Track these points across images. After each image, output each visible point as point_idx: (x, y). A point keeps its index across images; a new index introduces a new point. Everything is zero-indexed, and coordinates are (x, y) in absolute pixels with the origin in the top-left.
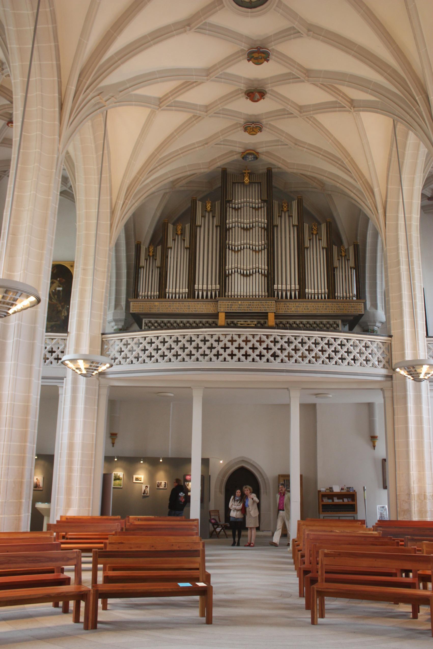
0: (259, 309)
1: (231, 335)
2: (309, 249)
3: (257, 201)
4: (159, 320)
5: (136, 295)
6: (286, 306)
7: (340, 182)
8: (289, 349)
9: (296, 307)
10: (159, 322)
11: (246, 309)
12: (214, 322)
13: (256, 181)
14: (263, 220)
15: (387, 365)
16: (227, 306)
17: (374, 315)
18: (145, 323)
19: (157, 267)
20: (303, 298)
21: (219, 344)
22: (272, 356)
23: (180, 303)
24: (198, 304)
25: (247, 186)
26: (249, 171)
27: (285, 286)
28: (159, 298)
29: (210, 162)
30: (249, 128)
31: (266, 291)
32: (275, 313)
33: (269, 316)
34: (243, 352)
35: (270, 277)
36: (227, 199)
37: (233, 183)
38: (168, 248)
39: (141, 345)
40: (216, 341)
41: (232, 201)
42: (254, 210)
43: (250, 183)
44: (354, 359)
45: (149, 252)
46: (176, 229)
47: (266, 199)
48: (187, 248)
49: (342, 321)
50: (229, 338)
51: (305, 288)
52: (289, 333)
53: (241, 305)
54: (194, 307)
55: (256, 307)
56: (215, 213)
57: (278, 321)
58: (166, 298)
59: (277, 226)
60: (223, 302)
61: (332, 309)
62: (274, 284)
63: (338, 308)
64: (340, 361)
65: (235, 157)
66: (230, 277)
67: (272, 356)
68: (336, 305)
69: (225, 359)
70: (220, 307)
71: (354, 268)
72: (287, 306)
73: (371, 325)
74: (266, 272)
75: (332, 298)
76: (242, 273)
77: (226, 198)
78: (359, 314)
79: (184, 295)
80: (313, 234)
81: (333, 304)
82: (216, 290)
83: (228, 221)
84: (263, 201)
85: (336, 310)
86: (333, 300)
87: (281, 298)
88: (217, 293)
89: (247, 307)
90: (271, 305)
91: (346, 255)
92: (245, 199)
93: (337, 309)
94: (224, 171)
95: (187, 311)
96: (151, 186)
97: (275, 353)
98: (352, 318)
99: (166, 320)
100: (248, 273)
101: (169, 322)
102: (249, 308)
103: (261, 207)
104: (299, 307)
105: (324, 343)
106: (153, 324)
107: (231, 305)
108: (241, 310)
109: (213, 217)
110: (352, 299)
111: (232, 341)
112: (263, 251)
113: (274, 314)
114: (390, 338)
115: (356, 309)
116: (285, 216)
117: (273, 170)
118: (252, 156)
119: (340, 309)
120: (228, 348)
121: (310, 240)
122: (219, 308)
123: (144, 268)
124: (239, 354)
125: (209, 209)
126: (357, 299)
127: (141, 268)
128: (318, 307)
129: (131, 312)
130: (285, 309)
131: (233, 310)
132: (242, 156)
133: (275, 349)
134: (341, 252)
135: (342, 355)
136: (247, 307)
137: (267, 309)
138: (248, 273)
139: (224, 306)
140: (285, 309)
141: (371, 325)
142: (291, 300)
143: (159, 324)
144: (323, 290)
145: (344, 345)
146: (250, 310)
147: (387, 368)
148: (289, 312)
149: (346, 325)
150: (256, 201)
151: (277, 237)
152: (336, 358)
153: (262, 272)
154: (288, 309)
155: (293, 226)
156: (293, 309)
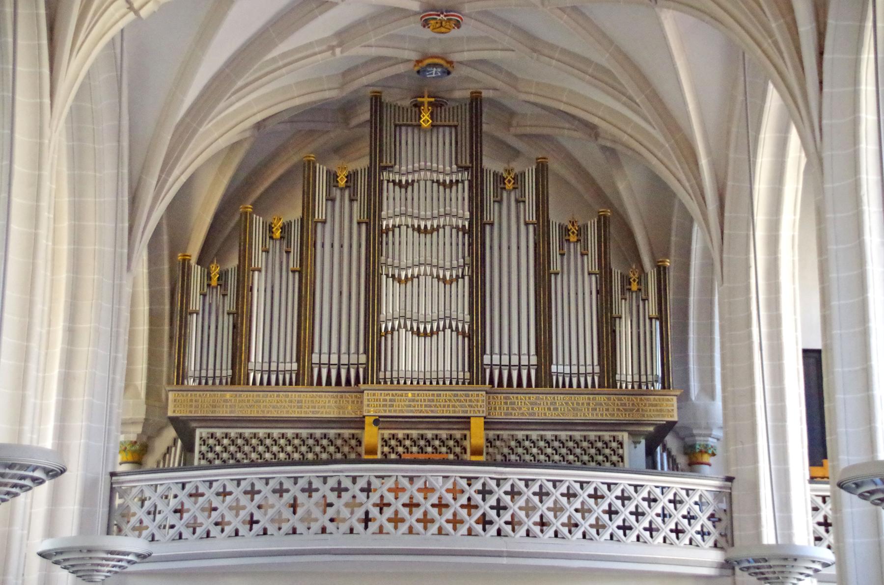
0: (451, 409)
1: (394, 479)
2: (559, 277)
3: (448, 168)
4: (233, 432)
5: (181, 377)
6: (509, 401)
7: (629, 131)
8: (515, 507)
9: (531, 404)
10: (233, 435)
11: (423, 409)
12: (353, 436)
13: (447, 123)
14: (461, 212)
15: (722, 542)
16: (382, 403)
17: (707, 412)
18: (201, 438)
19: (229, 314)
20: (545, 386)
21: (368, 497)
22: (477, 522)
23: (281, 394)
24: (320, 397)
25: (425, 131)
26: (433, 100)
27: (507, 357)
28: (233, 383)
29: (344, 74)
30: (433, 22)
31: (466, 369)
32: (485, 418)
33: (472, 425)
34: (419, 513)
35: (475, 338)
36: (384, 164)
37: (396, 126)
38: (253, 271)
39: (214, 514)
40: (362, 490)
41: (392, 167)
42: (441, 188)
43: (433, 126)
44: (650, 529)
45: (210, 278)
46: (271, 228)
47: (468, 164)
48: (294, 271)
49: (632, 434)
50: (390, 483)
51: (551, 363)
52: (514, 475)
53: (413, 400)
54: (311, 404)
55: (444, 406)
56: (355, 193)
57: (491, 434)
58: (248, 384)
59: (492, 225)
60: (374, 395)
61: (607, 410)
62: (484, 352)
63: (621, 408)
64: (621, 532)
65: (402, 68)
66: (389, 336)
67: (477, 522)
68: (617, 402)
69: (381, 528)
70: (368, 405)
71: (657, 319)
72: (511, 404)
73: (700, 435)
74: (466, 327)
75: (608, 387)
76: (415, 329)
77: (381, 161)
78: (668, 422)
79: (288, 376)
80: (568, 241)
81: (609, 399)
82: (358, 364)
83: (384, 213)
84: (462, 168)
85: (616, 412)
86: (611, 390)
87: (498, 386)
88: (361, 371)
89: (426, 406)
90: (478, 401)
91: (640, 290)
92: (422, 163)
93: (618, 410)
94: (376, 97)
95: (295, 414)
96: (216, 135)
97: (484, 515)
98: (651, 429)
99: (247, 432)
100: (428, 331)
101: (255, 436)
102: (430, 406)
103: (457, 181)
104: (536, 404)
105: (587, 493)
106: (219, 441)
107: (391, 400)
108: (412, 411)
109: (351, 200)
110: (653, 385)
111: (397, 490)
112: (460, 281)
113: (483, 420)
114: (729, 484)
115: (661, 410)
116: (509, 198)
117: (485, 94)
118: (439, 70)
119: (625, 410)
120: (389, 505)
121: (562, 255)
122: (365, 408)
123: (197, 314)
124: (412, 519)
125: (342, 183)
126: (663, 387)
127: (191, 314)
128: (578, 404)
129: (170, 414)
130: (508, 409)
131: (395, 411)
132: (417, 68)
133: (486, 507)
134: (630, 284)
135: (624, 520)
136: (426, 406)
137: (469, 409)
138: (428, 331)
139: (374, 402)
140: (508, 409)
141: (700, 435)
142: (520, 390)
143: (233, 441)
144: (589, 369)
145: (629, 498)
146: (432, 411)
147: (722, 548)
148: (516, 416)
149: (639, 442)
150: (446, 169)
151: (491, 248)
152: (612, 527)
153: (457, 327)
154: (513, 409)
155: (527, 224)
156: (524, 409)
